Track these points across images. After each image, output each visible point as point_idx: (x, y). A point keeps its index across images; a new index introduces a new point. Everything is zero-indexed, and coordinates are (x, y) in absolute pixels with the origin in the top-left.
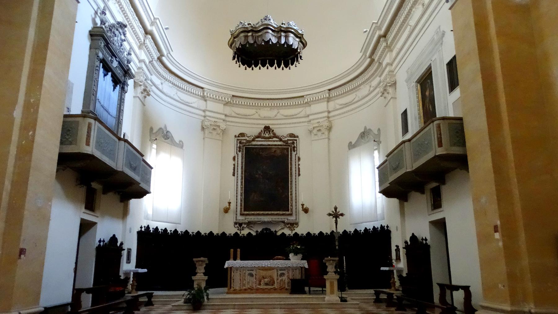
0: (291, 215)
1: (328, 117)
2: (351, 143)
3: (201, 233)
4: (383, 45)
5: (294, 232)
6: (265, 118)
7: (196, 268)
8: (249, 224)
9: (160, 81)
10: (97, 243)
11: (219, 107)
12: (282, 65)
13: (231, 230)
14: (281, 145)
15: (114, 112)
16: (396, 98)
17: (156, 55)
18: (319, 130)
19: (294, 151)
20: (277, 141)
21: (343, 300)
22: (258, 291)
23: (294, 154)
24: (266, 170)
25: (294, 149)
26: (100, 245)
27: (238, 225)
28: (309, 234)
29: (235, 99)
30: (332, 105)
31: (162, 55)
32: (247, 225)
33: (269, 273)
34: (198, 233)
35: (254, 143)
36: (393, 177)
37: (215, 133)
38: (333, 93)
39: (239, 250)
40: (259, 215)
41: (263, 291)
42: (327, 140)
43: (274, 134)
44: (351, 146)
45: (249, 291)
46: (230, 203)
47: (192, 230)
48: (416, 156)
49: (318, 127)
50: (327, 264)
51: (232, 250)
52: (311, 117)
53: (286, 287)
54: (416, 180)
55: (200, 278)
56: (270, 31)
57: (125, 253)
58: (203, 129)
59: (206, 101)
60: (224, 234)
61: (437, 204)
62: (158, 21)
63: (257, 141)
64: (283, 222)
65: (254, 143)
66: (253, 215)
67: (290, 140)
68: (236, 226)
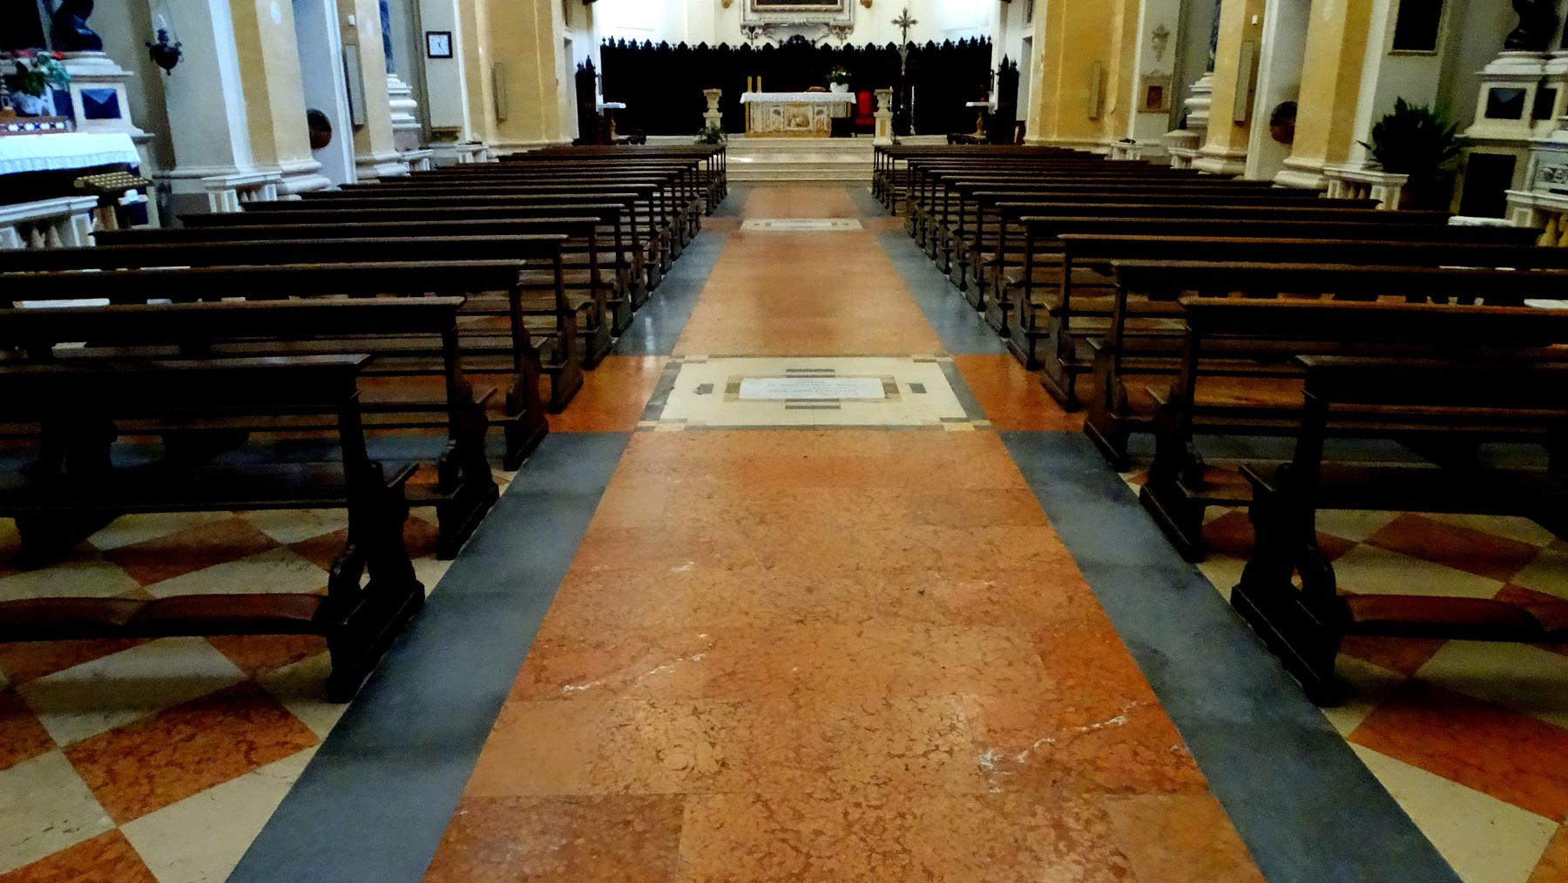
0: (840, 11)
10: (576, 69)
13: (736, 40)
22: (786, 133)
33: (803, 109)
34: (683, 45)
39: (759, 79)
40: (783, 11)
41: (794, 134)
47: (673, 42)
51: (750, 79)
55: (713, 116)
60: (724, 46)
64: (827, 24)
66: (774, 11)
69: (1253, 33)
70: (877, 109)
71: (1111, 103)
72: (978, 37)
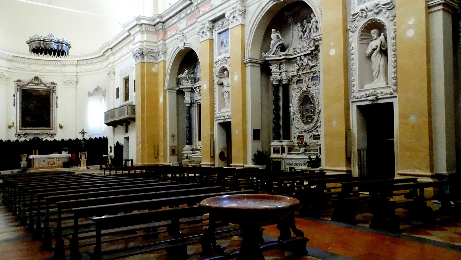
0: (52, 129)
1: (76, 76)
2: (89, 92)
5: (53, 139)
6: (34, 71)
12: (56, 55)
13: (13, 138)
21: (88, 168)
23: (54, 94)
25: (54, 92)
29: (14, 58)
30: (79, 68)
33: (53, 160)
35: (28, 86)
43: (41, 82)
44: (90, 94)
46: (13, 123)
48: (120, 115)
51: (34, 151)
52: (65, 74)
56: (53, 43)
60: (9, 141)
61: (127, 131)
64: (47, 134)
65: (28, 86)
69: (212, 136)
71: (161, 153)
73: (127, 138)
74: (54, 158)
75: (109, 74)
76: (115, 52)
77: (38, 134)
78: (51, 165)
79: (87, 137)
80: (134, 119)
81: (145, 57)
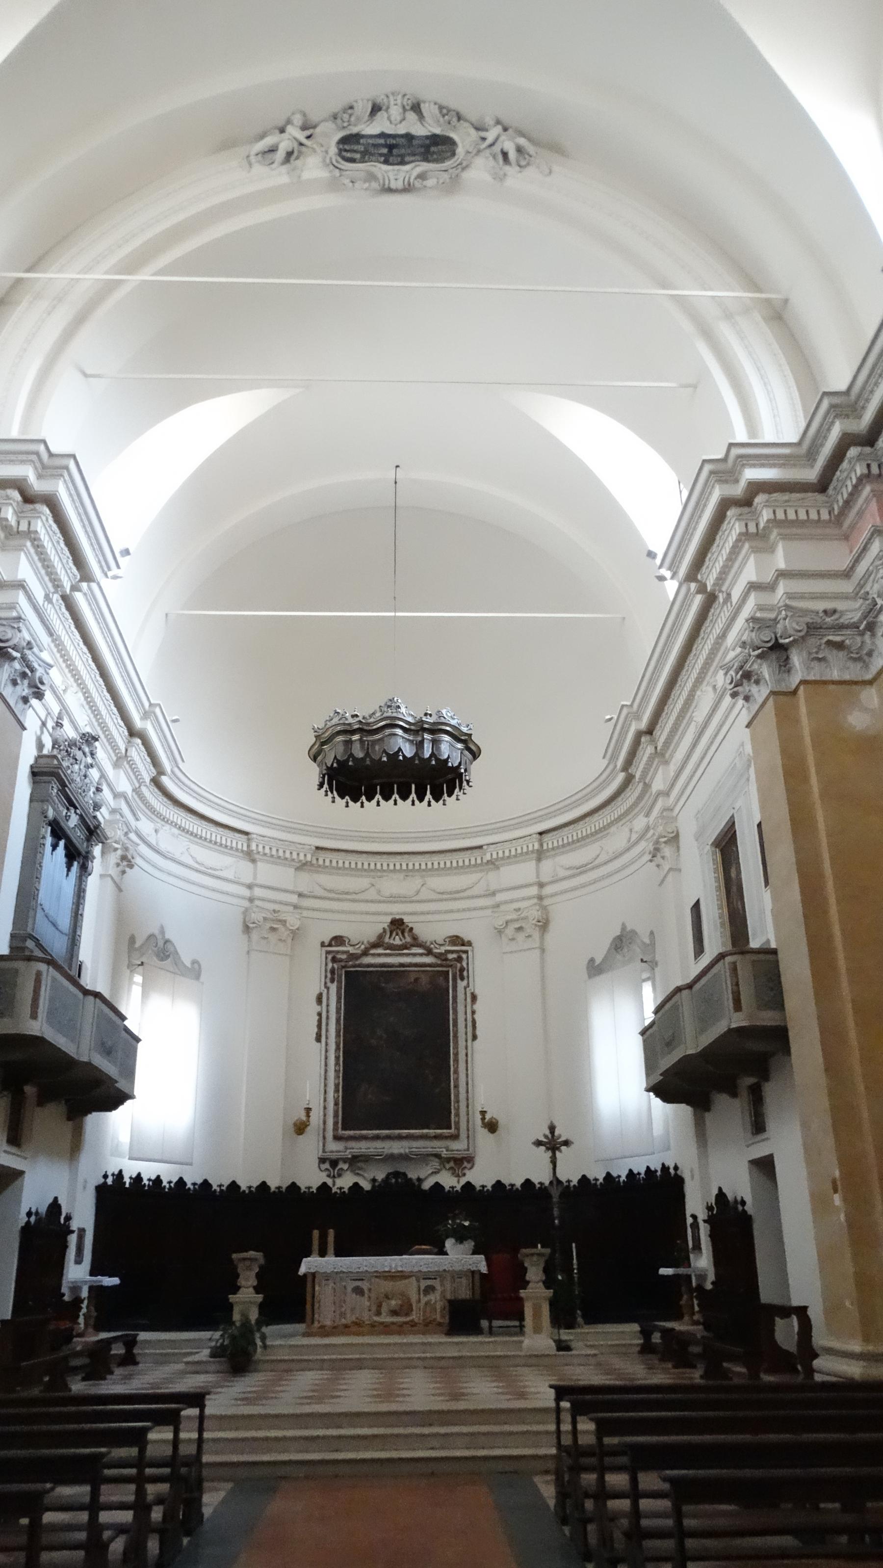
0: (455, 1137)
1: (540, 898)
2: (592, 960)
3: (239, 1187)
4: (646, 750)
5: (463, 1181)
7: (238, 1276)
8: (356, 1162)
9: (152, 825)
10: (23, 1219)
11: (284, 876)
12: (428, 796)
13: (311, 1177)
14: (429, 965)
15: (65, 922)
16: (680, 870)
17: (147, 772)
18: (520, 929)
19: (462, 979)
20: (421, 955)
21: (563, 1346)
22: (376, 1328)
23: (461, 985)
24: (395, 1027)
25: (462, 974)
26: (28, 1223)
27: (327, 1165)
28: (499, 1184)
29: (322, 855)
30: (548, 867)
31: (161, 772)
32: (351, 1165)
33: (400, 1285)
34: (234, 1185)
36: (667, 1062)
37: (273, 937)
38: (550, 841)
39: (331, 1233)
40: (377, 1138)
41: (387, 1329)
42: (537, 952)
43: (415, 938)
44: (595, 969)
45: (354, 1329)
46: (308, 1110)
47: (219, 1180)
48: (704, 1022)
49: (517, 920)
50: (526, 1265)
51: (316, 1233)
52: (500, 897)
53: (439, 1319)
54: (715, 1068)
55: (246, 1299)
56: (399, 732)
57: (73, 1239)
58: (247, 929)
59: (253, 861)
60: (294, 1187)
61: (758, 1127)
62: (158, 710)
63: (373, 955)
64: (437, 1156)
67: (452, 952)
68: (324, 1166)
70: (525, 1284)
72: (656, 1166)
73: (765, 1167)
74: (402, 1276)
75: (656, 852)
76: (667, 743)
77: (404, 1158)
78: (394, 1313)
79: (570, 1170)
80: (780, 1037)
81: (796, 659)
